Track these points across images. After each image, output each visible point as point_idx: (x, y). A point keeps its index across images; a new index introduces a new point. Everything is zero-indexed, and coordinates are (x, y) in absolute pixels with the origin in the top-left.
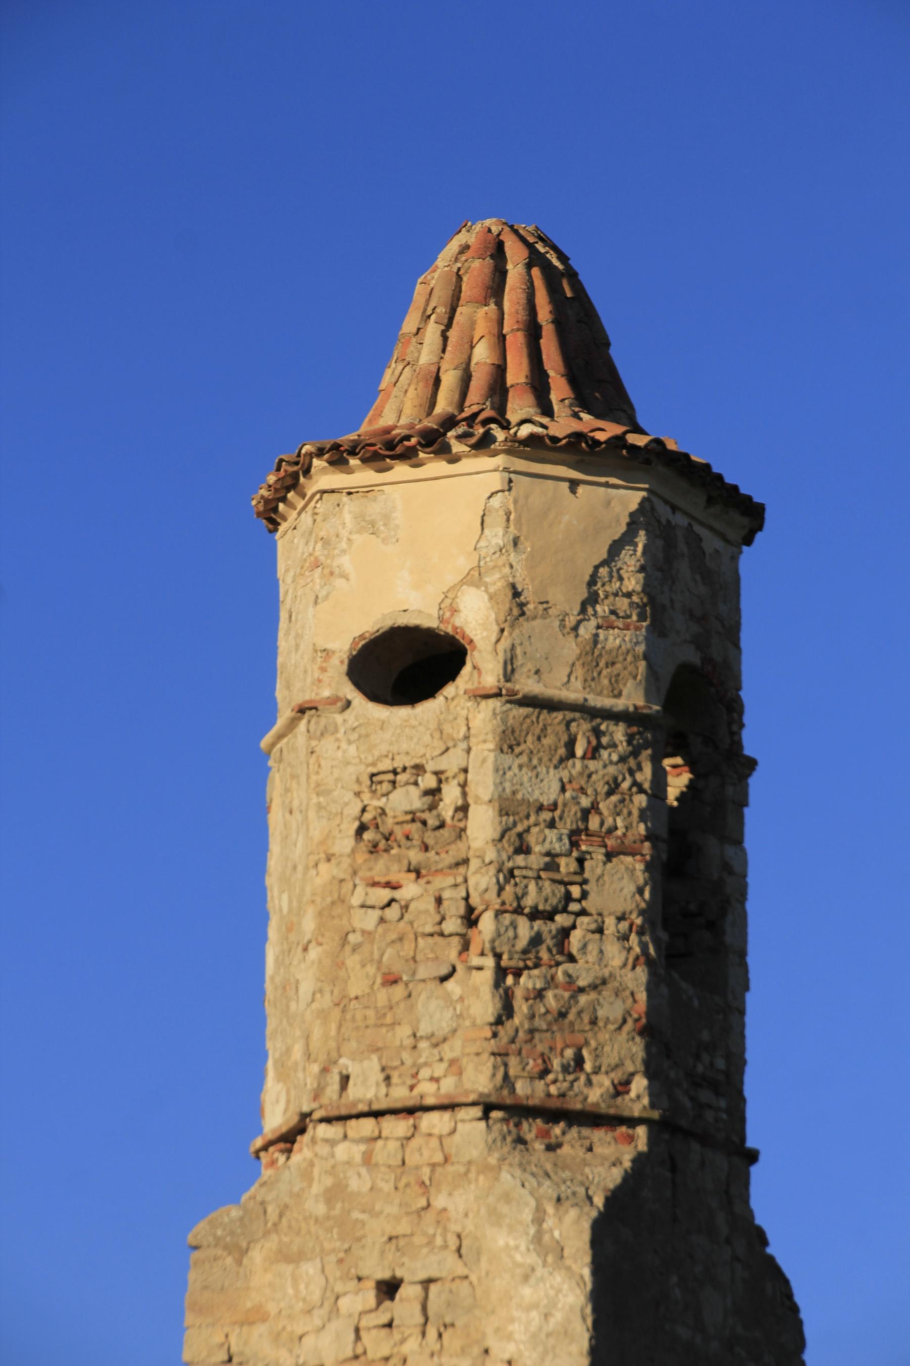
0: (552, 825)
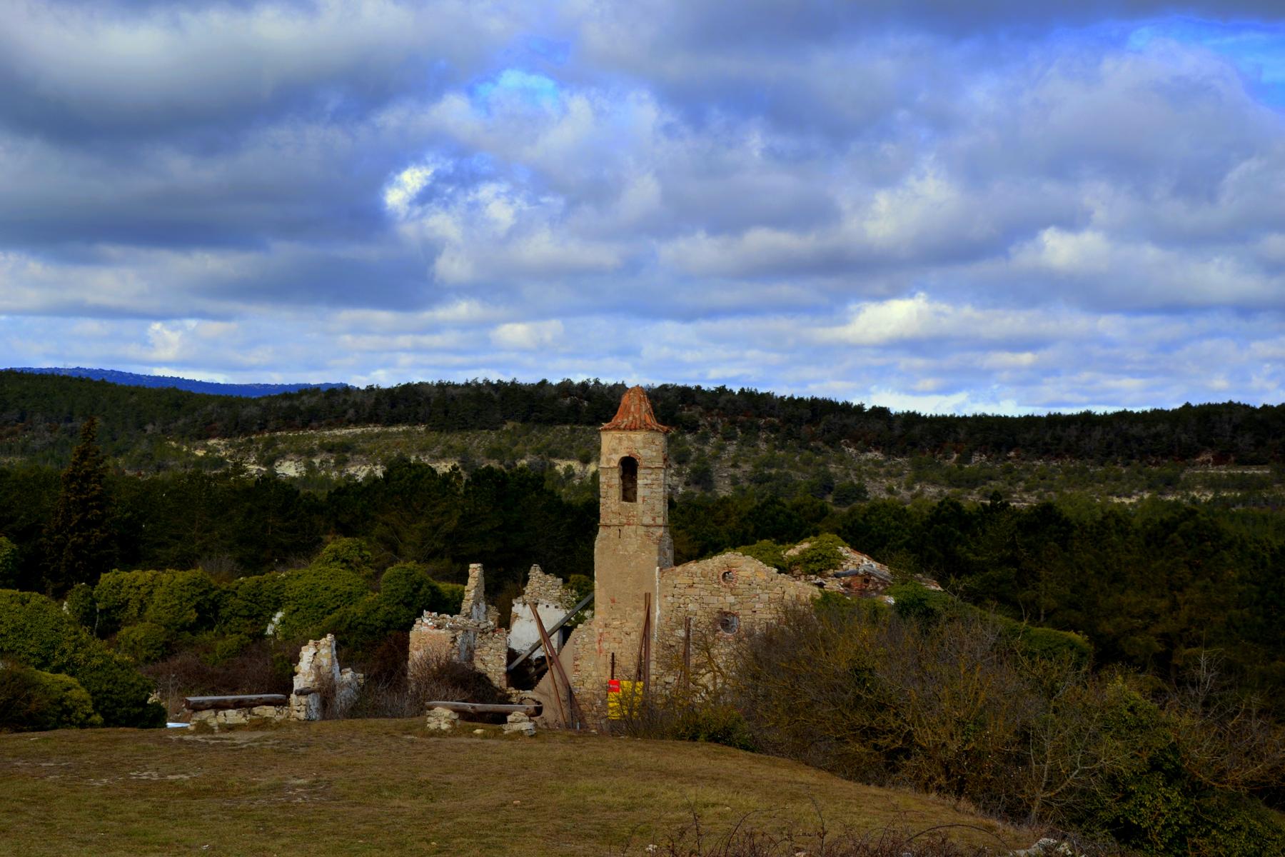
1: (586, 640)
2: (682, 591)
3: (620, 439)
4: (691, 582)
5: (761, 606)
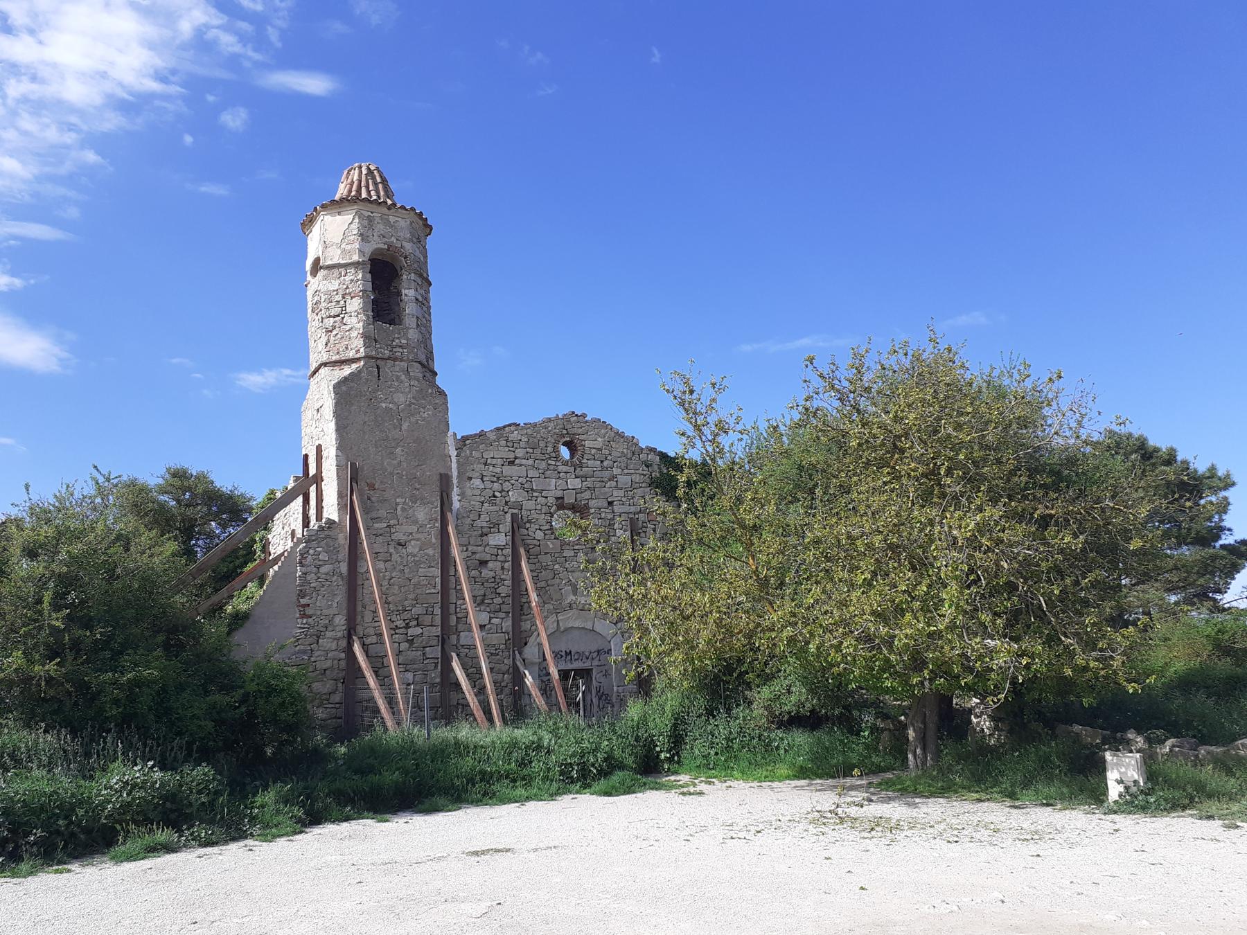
0: (337, 294)
1: (324, 556)
2: (498, 470)
4: (512, 455)
5: (621, 493)
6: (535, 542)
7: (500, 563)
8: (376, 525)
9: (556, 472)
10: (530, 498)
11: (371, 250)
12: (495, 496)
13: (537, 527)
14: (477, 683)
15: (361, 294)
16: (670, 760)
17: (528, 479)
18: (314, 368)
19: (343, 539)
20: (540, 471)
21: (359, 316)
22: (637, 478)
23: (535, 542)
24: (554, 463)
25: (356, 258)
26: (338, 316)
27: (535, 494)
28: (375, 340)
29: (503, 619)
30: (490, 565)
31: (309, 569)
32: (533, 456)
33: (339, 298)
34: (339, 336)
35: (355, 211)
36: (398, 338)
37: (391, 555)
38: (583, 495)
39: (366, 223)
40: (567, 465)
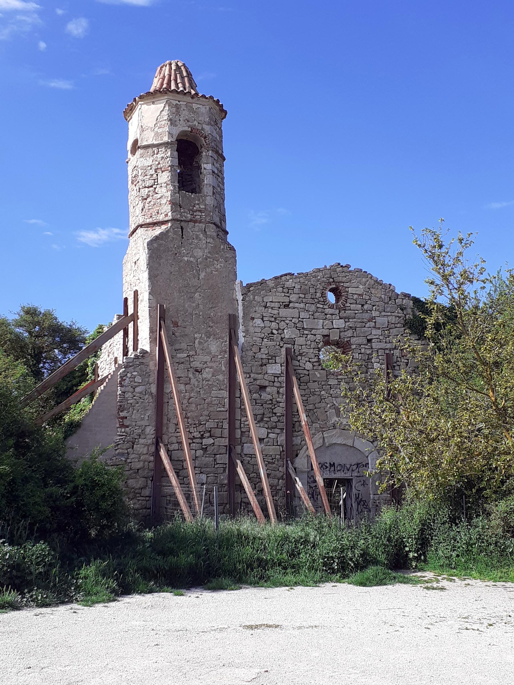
0: (151, 169)
1: (138, 379)
2: (276, 312)
3: (177, 107)
4: (287, 300)
5: (379, 332)
6: (305, 372)
7: (276, 388)
8: (179, 355)
9: (324, 314)
10: (301, 335)
11: (178, 132)
12: (272, 333)
13: (307, 359)
14: (257, 485)
15: (169, 168)
16: (417, 559)
17: (300, 319)
18: (133, 229)
19: (153, 366)
20: (310, 313)
21: (168, 186)
22: (393, 320)
23: (305, 372)
24: (322, 306)
25: (166, 139)
26: (152, 186)
27: (306, 332)
28: (180, 205)
29: (278, 434)
30: (268, 389)
31: (127, 389)
32: (304, 300)
33: (152, 172)
34: (152, 203)
35: (165, 100)
36: (198, 204)
37: (190, 379)
38: (346, 333)
39: (174, 110)
40: (333, 308)
